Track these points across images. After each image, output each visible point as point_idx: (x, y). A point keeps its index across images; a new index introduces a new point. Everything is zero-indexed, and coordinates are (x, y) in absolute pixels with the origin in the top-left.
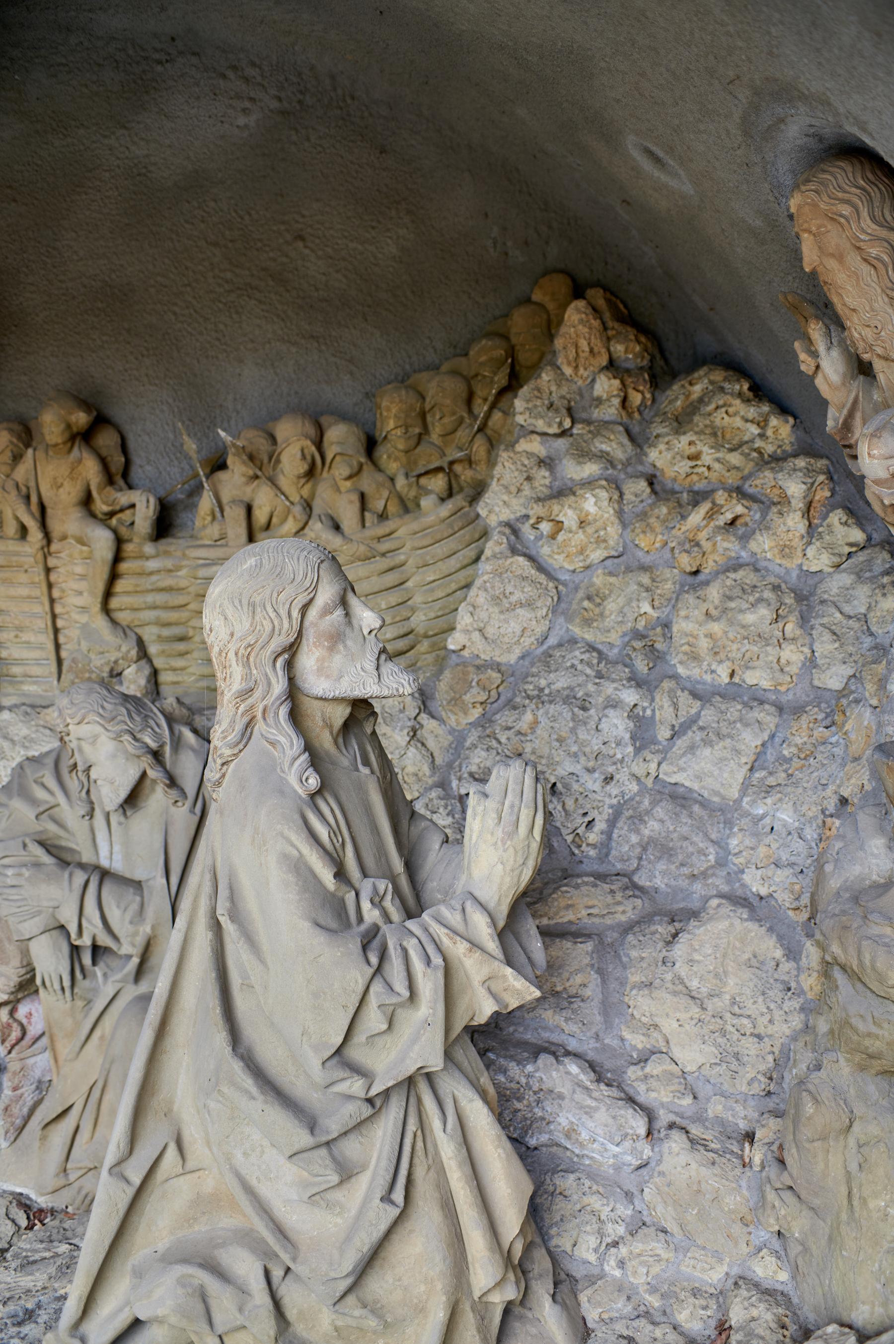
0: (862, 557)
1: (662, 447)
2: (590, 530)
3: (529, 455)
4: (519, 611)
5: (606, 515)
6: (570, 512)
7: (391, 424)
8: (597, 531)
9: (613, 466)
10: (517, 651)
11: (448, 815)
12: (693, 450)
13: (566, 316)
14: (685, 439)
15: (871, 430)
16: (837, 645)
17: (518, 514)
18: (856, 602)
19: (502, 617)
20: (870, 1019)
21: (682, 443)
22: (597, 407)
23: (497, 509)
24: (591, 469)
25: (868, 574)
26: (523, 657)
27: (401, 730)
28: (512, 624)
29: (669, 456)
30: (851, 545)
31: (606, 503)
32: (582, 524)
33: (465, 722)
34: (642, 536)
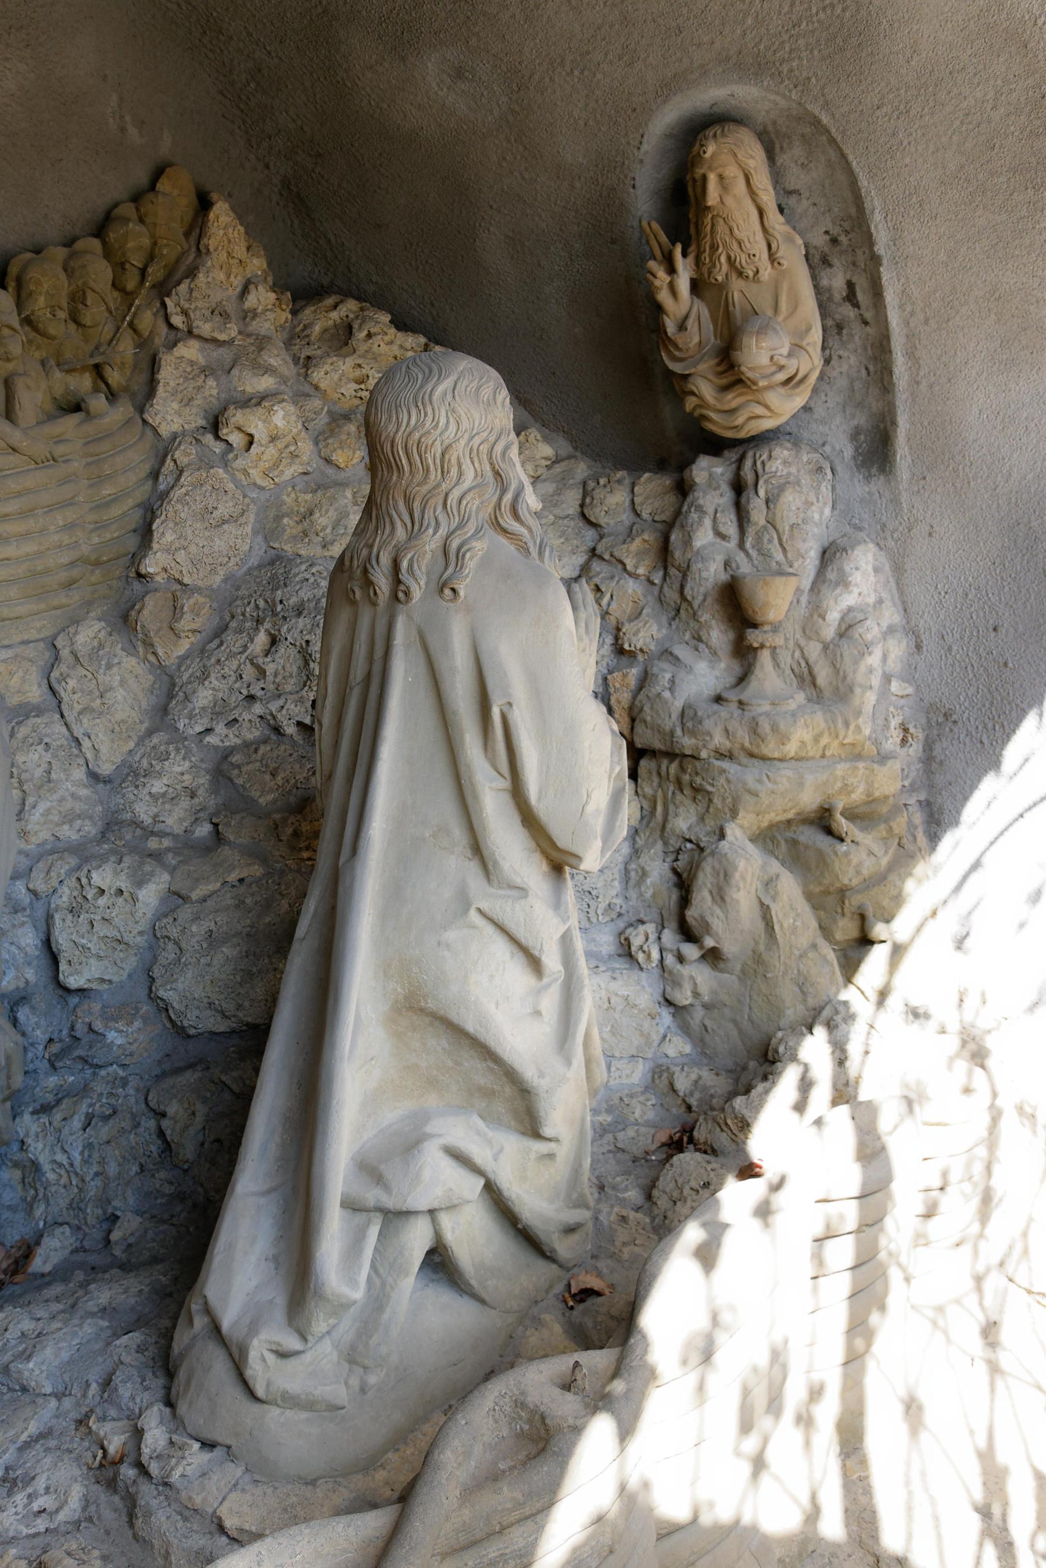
0: (558, 469)
1: (327, 367)
2: (280, 444)
3: (192, 363)
4: (226, 526)
5: (295, 430)
6: (260, 424)
7: (41, 301)
8: (287, 447)
9: (285, 383)
10: (222, 573)
11: (184, 759)
12: (358, 373)
13: (212, 215)
14: (350, 361)
15: (756, 329)
16: (562, 540)
17: (193, 425)
18: (564, 506)
19: (207, 534)
20: (765, 778)
21: (346, 365)
22: (253, 318)
23: (169, 418)
24: (265, 383)
25: (571, 482)
26: (225, 581)
27: (109, 667)
28: (218, 542)
29: (336, 377)
30: (546, 459)
31: (294, 418)
32: (273, 439)
33: (175, 654)
34: (339, 452)
